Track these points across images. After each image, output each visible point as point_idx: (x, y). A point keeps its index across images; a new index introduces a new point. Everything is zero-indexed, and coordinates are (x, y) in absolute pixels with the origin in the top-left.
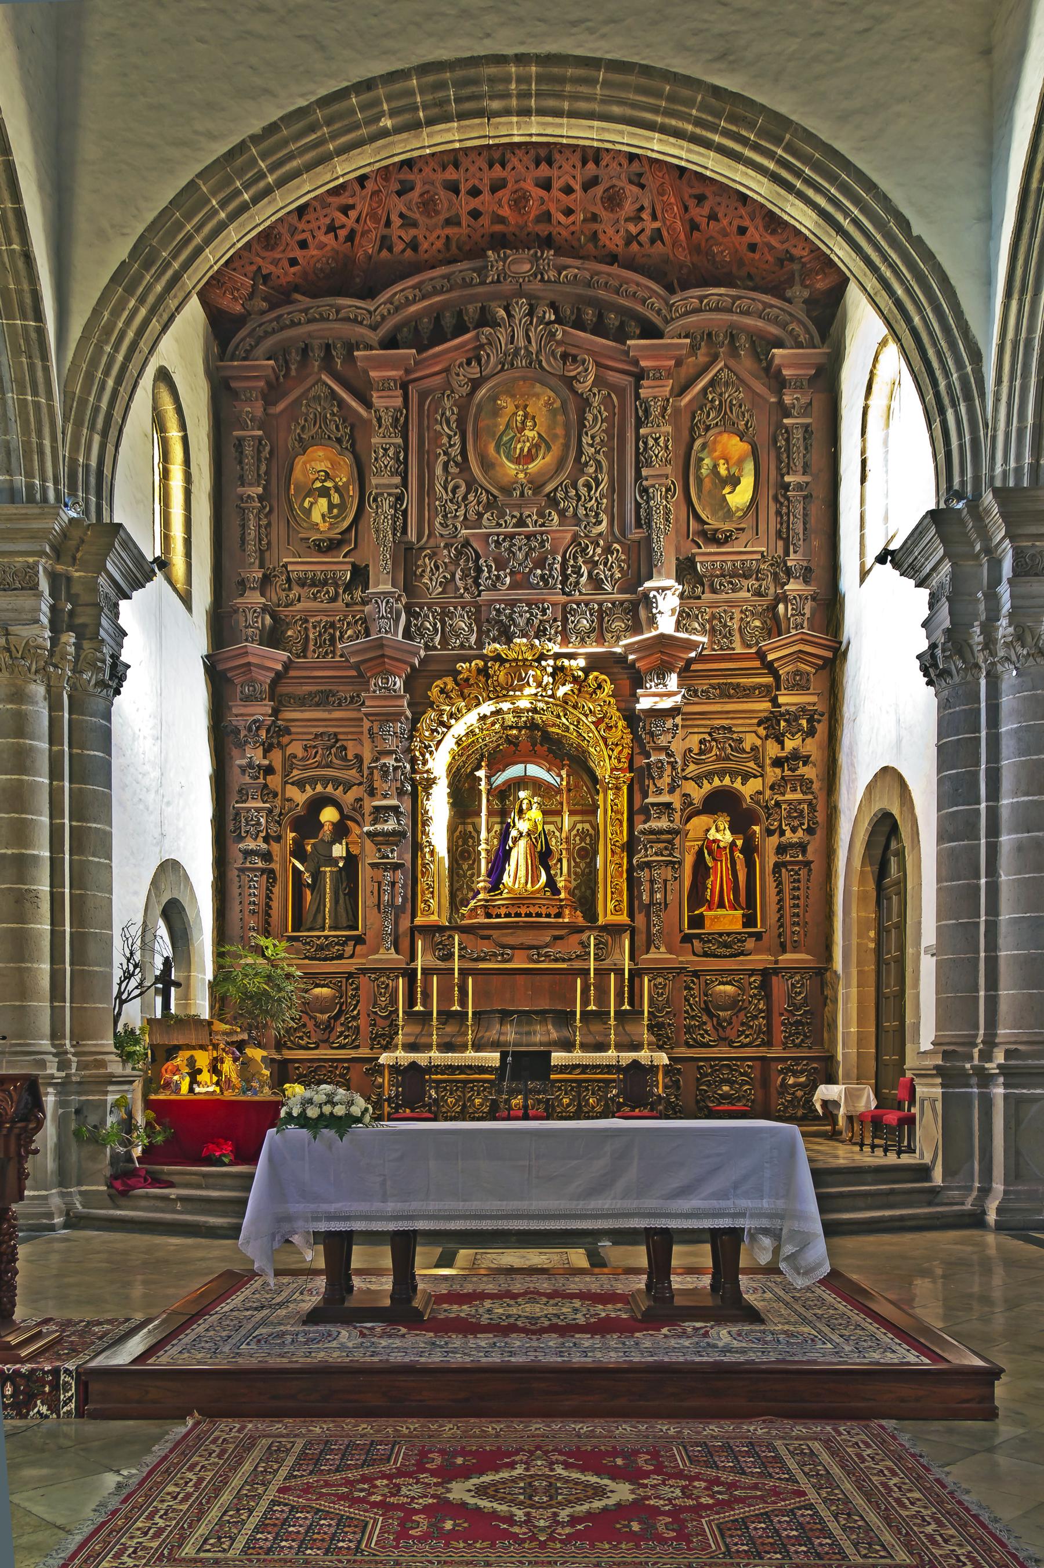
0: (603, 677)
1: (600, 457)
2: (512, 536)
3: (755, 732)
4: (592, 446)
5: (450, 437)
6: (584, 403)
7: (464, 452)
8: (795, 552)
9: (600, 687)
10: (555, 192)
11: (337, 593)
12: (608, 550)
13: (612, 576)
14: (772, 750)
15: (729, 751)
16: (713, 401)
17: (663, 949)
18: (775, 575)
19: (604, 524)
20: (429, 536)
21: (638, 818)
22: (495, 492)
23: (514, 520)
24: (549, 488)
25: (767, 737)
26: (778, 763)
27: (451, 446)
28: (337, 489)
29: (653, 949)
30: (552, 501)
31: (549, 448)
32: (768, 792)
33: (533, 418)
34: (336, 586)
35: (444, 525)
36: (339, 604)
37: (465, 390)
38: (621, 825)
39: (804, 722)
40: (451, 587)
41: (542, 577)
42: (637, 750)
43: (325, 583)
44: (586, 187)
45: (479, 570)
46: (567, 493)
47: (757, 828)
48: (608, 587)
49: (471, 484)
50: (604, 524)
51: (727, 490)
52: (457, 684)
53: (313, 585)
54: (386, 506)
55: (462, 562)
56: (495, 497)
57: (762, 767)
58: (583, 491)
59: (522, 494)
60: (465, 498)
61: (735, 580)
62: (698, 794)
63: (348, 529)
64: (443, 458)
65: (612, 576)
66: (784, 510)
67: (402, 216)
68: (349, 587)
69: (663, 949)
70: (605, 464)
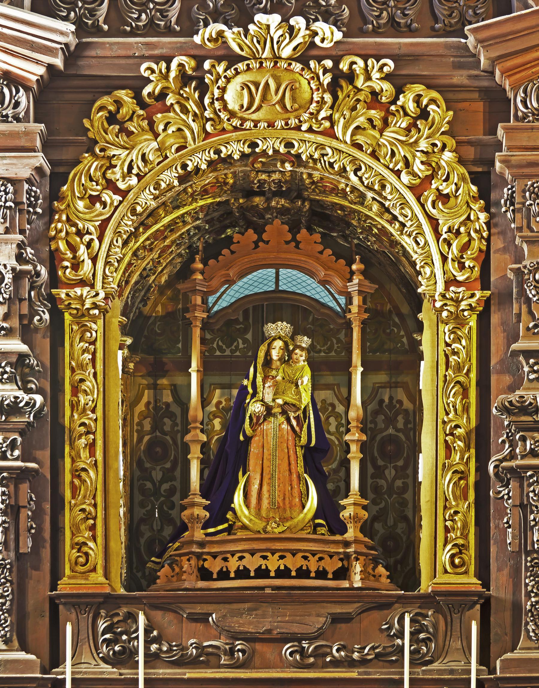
0: (435, 94)
9: (424, 114)
52: (142, 104)
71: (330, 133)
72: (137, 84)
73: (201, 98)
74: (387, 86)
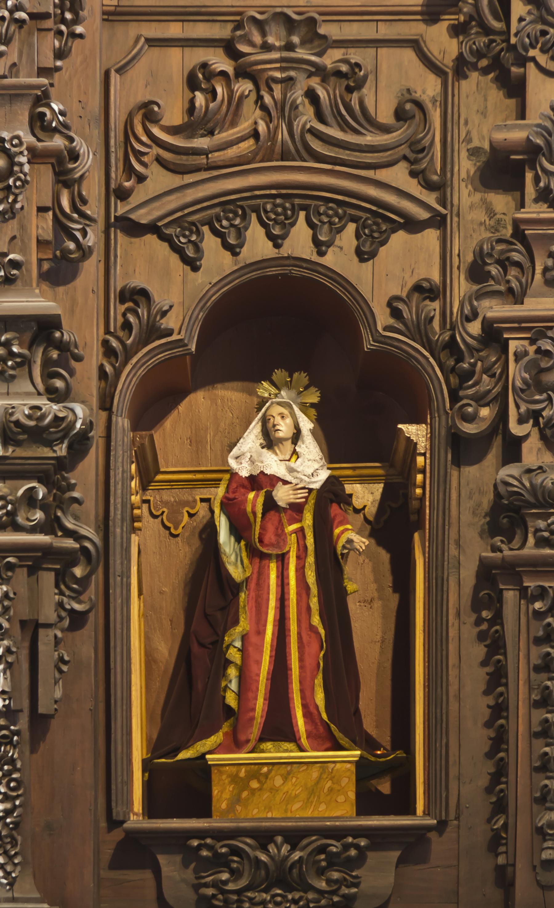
3: (415, 45)
25: (461, 68)
26: (503, 170)
32: (461, 287)
57: (441, 188)
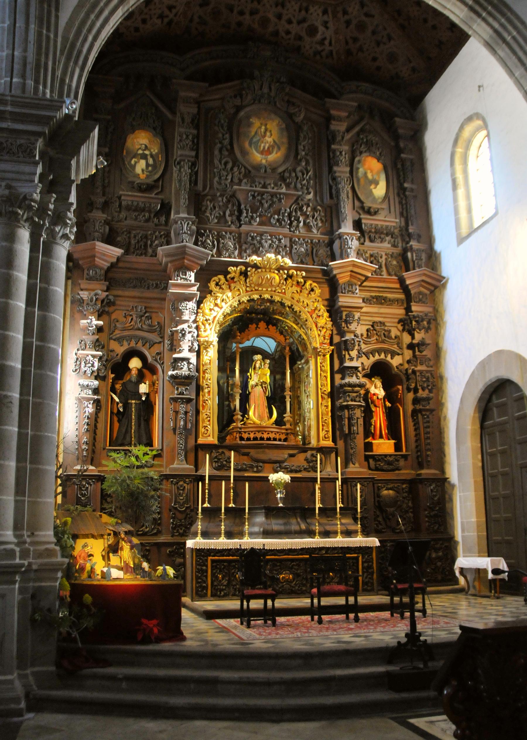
0: (315, 284)
1: (308, 158)
2: (262, 194)
3: (397, 327)
4: (304, 150)
5: (223, 135)
6: (298, 128)
7: (231, 144)
8: (412, 225)
9: (312, 290)
10: (283, 22)
11: (150, 216)
12: (314, 209)
13: (317, 225)
14: (407, 339)
15: (383, 338)
16: (362, 139)
17: (357, 465)
18: (402, 235)
19: (312, 194)
20: (210, 188)
21: (338, 377)
22: (250, 169)
23: (261, 185)
24: (280, 170)
25: (403, 330)
27: (224, 139)
28: (152, 156)
29: (351, 465)
30: (283, 179)
31: (279, 149)
33: (270, 131)
34: (150, 212)
35: (220, 183)
36: (150, 224)
37: (232, 111)
38: (327, 380)
39: (425, 323)
40: (222, 221)
41: (278, 220)
42: (335, 332)
43: (143, 210)
44: (299, 23)
45: (240, 212)
46: (290, 174)
47: (400, 387)
48: (315, 231)
49: (235, 162)
50: (312, 194)
51: (372, 187)
52: (227, 280)
53: (135, 210)
54: (186, 167)
55: (230, 206)
56: (250, 172)
58: (300, 174)
59: (266, 171)
60: (232, 169)
61: (382, 236)
62: (368, 362)
63: (158, 180)
64: (219, 145)
65: (317, 225)
66: (404, 202)
67: (200, 17)
68: (157, 214)
69: (357, 465)
70: (311, 162)
71: (285, 293)
72: (226, 273)
73: (246, 280)
74: (302, 280)
